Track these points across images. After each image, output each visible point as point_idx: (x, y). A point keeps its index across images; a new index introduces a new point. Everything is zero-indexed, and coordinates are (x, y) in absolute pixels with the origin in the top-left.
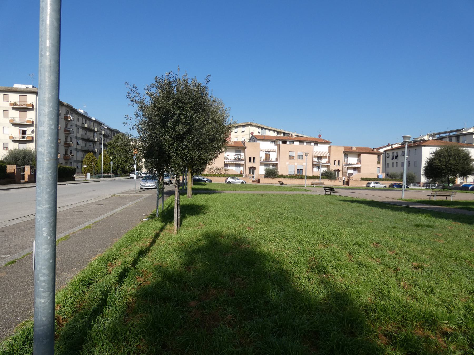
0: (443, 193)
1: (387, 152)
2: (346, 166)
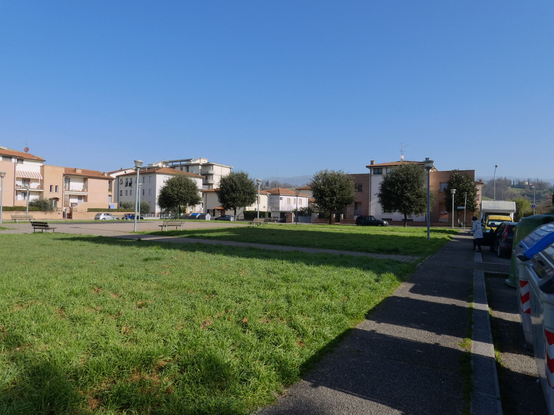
0: (174, 223)
1: (120, 178)
2: (68, 193)
